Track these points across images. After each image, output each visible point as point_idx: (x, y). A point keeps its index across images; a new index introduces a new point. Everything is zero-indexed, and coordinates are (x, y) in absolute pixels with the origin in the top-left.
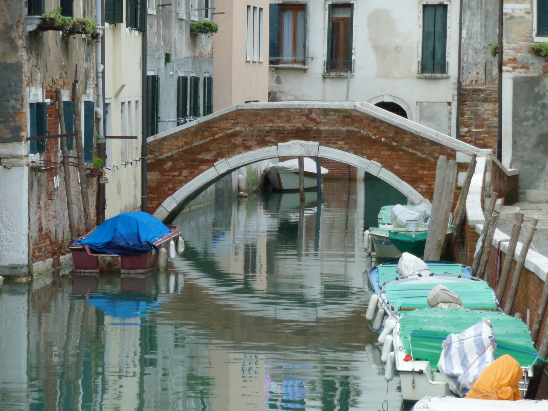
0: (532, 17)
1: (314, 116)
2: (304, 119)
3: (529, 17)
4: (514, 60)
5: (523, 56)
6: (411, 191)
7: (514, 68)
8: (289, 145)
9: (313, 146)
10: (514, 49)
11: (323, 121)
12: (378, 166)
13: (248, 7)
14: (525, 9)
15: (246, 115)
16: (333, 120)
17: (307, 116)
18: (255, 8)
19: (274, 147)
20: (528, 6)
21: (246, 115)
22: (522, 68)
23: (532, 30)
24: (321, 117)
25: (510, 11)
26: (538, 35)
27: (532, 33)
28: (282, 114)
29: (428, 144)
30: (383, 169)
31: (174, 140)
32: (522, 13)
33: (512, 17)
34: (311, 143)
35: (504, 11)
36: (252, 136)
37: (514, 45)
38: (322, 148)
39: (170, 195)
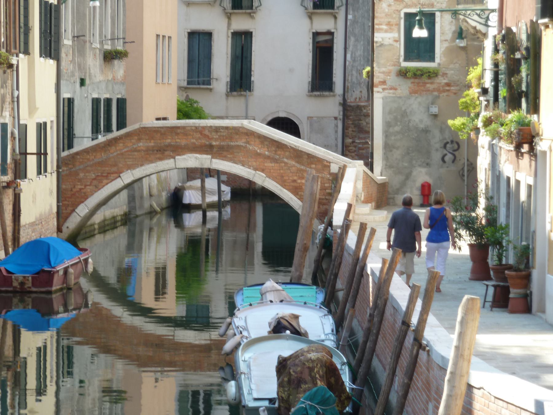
0: (400, 44)
1: (206, 132)
2: (198, 135)
3: (397, 45)
4: (384, 82)
5: (392, 80)
6: (291, 198)
7: (384, 89)
8: (185, 158)
9: (205, 159)
10: (383, 73)
11: (215, 137)
12: (262, 176)
13: (158, 36)
14: (394, 37)
15: (148, 132)
16: (223, 136)
17: (201, 133)
18: (164, 37)
19: (172, 160)
20: (396, 35)
21: (148, 132)
22: (391, 89)
23: (399, 56)
24: (213, 134)
25: (380, 40)
26: (407, 59)
27: (399, 59)
28: (179, 131)
29: (306, 156)
30: (267, 179)
31: (85, 154)
32: (391, 42)
33: (382, 45)
34: (205, 156)
35: (375, 39)
36: (153, 151)
37: (384, 69)
38: (214, 160)
39: (83, 202)
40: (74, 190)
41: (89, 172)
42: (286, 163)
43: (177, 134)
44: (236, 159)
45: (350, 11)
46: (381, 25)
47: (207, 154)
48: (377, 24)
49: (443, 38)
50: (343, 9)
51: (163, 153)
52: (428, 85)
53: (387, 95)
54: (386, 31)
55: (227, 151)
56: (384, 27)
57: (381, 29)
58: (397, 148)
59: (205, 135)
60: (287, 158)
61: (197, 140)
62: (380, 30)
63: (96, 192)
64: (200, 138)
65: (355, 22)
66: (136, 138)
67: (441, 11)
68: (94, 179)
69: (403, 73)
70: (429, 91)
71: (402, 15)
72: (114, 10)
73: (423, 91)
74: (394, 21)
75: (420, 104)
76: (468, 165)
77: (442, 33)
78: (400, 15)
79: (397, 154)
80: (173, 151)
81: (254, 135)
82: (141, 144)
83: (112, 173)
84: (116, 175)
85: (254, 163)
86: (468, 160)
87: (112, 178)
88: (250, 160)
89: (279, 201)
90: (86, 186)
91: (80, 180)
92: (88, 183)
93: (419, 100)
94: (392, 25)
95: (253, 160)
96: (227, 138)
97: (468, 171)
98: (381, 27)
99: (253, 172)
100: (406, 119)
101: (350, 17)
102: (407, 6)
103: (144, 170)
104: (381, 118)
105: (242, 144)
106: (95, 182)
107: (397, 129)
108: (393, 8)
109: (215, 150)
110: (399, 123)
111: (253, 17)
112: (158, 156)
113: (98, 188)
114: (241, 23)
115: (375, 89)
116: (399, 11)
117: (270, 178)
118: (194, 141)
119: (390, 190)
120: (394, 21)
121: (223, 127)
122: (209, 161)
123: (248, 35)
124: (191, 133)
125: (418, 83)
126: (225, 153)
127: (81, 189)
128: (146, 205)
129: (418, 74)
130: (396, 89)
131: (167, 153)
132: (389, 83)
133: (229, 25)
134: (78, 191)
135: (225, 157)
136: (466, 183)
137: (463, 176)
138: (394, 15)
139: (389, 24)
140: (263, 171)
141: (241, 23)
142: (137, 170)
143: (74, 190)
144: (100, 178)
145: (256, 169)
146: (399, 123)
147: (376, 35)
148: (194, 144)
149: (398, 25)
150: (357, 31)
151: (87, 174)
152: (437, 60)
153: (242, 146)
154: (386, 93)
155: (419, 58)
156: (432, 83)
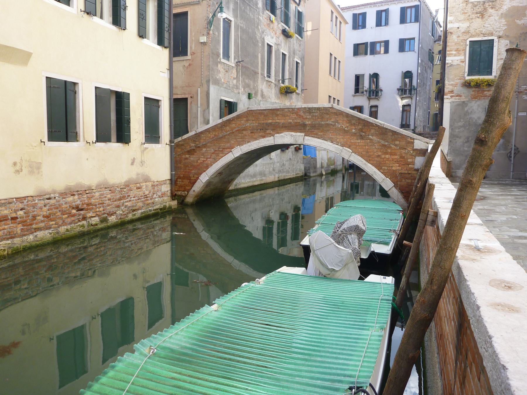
0: (465, 64)
1: (301, 113)
2: (294, 116)
3: (463, 64)
4: (452, 92)
5: (458, 89)
6: (375, 172)
7: (452, 97)
8: (282, 136)
9: (299, 136)
10: (452, 85)
11: (308, 117)
12: (349, 151)
13: (330, 97)
14: (461, 59)
15: (254, 114)
16: (315, 116)
17: (297, 113)
18: (334, 99)
19: (272, 137)
20: (463, 58)
21: (254, 114)
22: (457, 96)
23: (464, 72)
24: (307, 114)
25: (451, 62)
26: (468, 75)
27: (464, 74)
28: (278, 112)
29: (391, 134)
30: (353, 154)
31: (207, 133)
32: (458, 62)
33: (451, 65)
34: (299, 134)
35: (447, 62)
36: (257, 130)
37: (452, 82)
38: (306, 137)
39: (205, 171)
40: (199, 161)
41: (209, 147)
42: (371, 139)
43: (277, 115)
44: (325, 136)
45: (418, 96)
46: (452, 51)
47: (301, 132)
48: (448, 51)
49: (499, 57)
50: (415, 95)
51: (265, 132)
52: (486, 92)
53: (454, 100)
54: (455, 55)
55: (318, 129)
56: (454, 52)
57: (451, 54)
58: (460, 138)
59: (300, 115)
60: (372, 136)
61: (293, 120)
62: (450, 55)
63: (214, 163)
64: (295, 119)
65: (419, 101)
66: (245, 119)
67: (499, 37)
68: (213, 153)
69: (467, 85)
70: (486, 96)
71: (468, 43)
72: (292, 69)
73: (482, 96)
74: (461, 48)
75: (479, 106)
76: (515, 150)
77: (499, 54)
78: (466, 43)
79: (459, 142)
80: (273, 130)
81: (342, 114)
82: (248, 124)
83: (226, 149)
84: (228, 150)
85: (342, 140)
86: (515, 146)
87: (226, 152)
88: (338, 137)
89: (362, 173)
90: (207, 158)
91: (203, 154)
92: (209, 157)
93: (478, 103)
94: (460, 51)
95: (341, 137)
96: (318, 118)
97: (514, 154)
98: (451, 52)
99: (341, 148)
100: (468, 117)
101: (418, 99)
102: (472, 36)
103: (249, 146)
104: (449, 117)
105: (331, 123)
106: (214, 155)
107: (460, 124)
108: (461, 38)
109: (308, 128)
110: (462, 120)
111: (378, 100)
112: (261, 134)
113: (216, 161)
114: (373, 103)
115: (445, 97)
116: (466, 40)
117: (355, 153)
118: (291, 121)
119: (453, 166)
120: (461, 48)
121: (315, 108)
122: (302, 138)
123: (376, 106)
124: (289, 114)
125: (478, 91)
126: (316, 131)
127: (204, 161)
128: (319, 172)
129: (478, 85)
130: (461, 96)
131: (268, 131)
132: (455, 92)
133: (369, 103)
134: (201, 163)
135: (317, 134)
136: (512, 162)
137: (511, 157)
138: (462, 44)
139: (457, 50)
140: (349, 147)
141: (373, 103)
142: (244, 146)
143: (199, 161)
144: (217, 152)
145: (343, 146)
146: (462, 120)
147: (447, 58)
148: (290, 123)
149: (465, 50)
150: (420, 105)
151: (208, 149)
152: (494, 74)
153: (332, 124)
154: (453, 99)
155: (479, 73)
156: (488, 91)
